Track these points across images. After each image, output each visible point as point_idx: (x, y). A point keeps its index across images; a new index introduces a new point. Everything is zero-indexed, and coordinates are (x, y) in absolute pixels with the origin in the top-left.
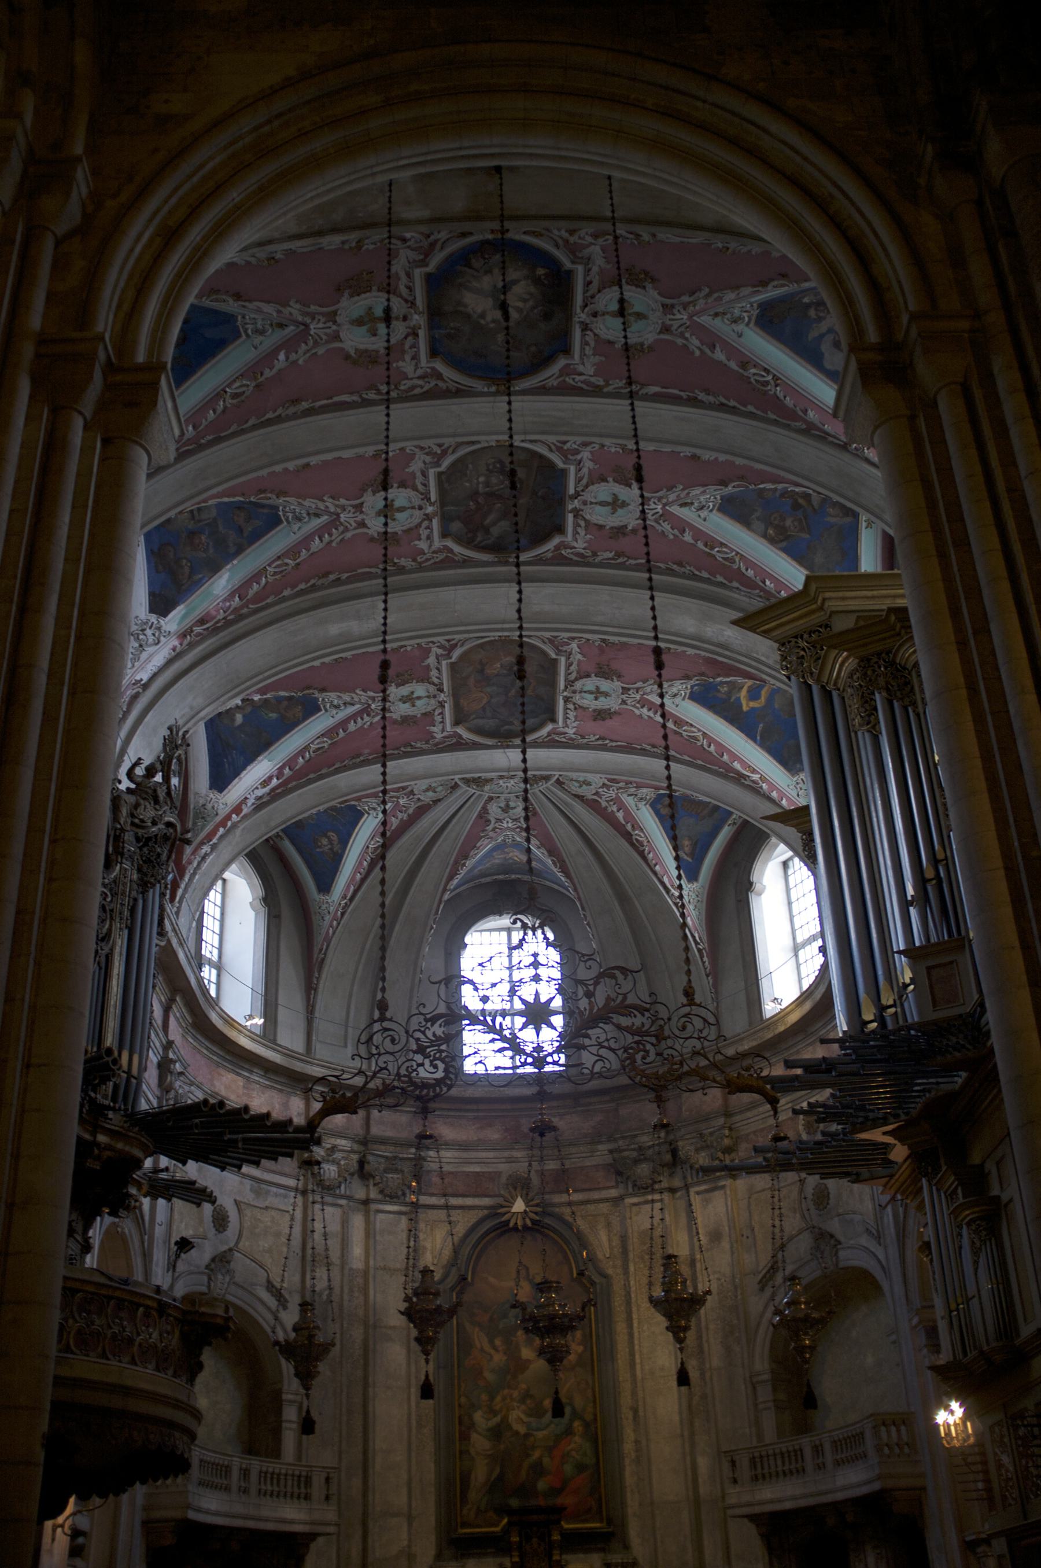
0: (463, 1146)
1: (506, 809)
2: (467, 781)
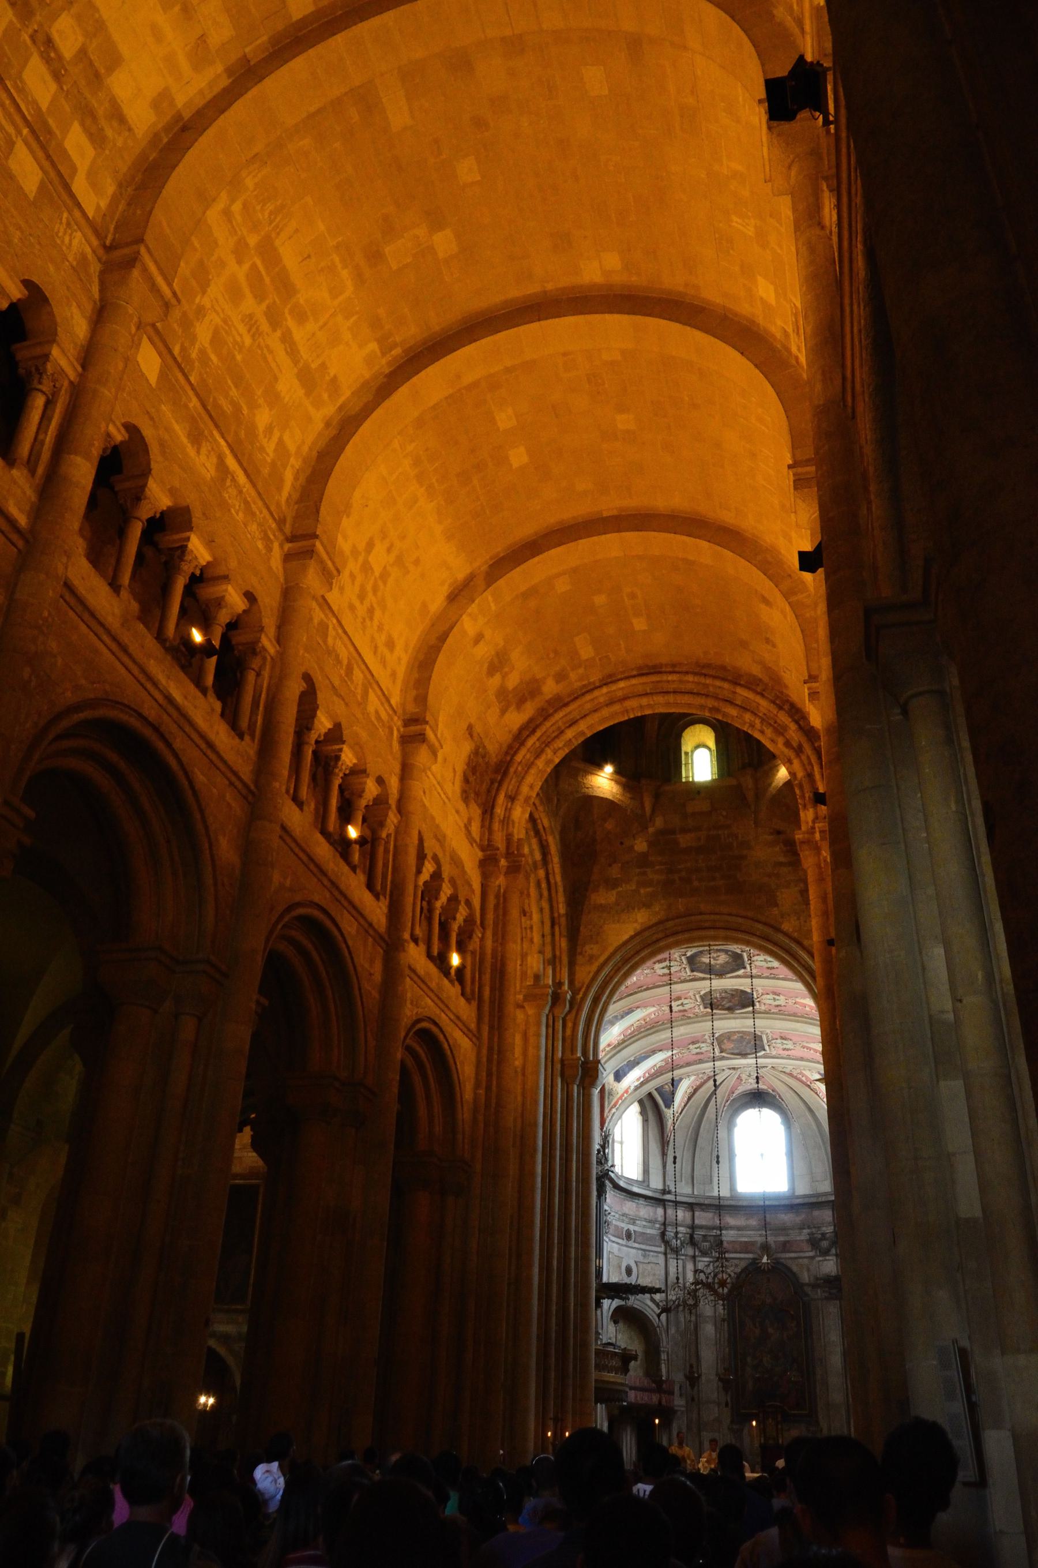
0: (739, 1228)
1: (750, 1076)
2: (730, 1069)
